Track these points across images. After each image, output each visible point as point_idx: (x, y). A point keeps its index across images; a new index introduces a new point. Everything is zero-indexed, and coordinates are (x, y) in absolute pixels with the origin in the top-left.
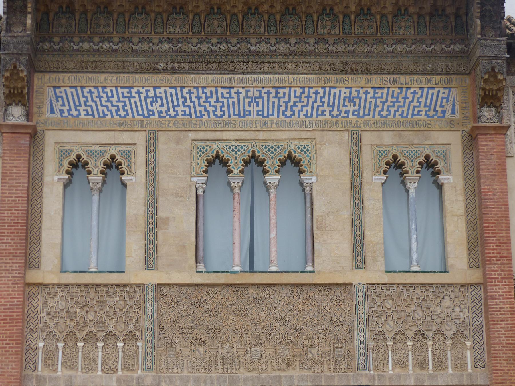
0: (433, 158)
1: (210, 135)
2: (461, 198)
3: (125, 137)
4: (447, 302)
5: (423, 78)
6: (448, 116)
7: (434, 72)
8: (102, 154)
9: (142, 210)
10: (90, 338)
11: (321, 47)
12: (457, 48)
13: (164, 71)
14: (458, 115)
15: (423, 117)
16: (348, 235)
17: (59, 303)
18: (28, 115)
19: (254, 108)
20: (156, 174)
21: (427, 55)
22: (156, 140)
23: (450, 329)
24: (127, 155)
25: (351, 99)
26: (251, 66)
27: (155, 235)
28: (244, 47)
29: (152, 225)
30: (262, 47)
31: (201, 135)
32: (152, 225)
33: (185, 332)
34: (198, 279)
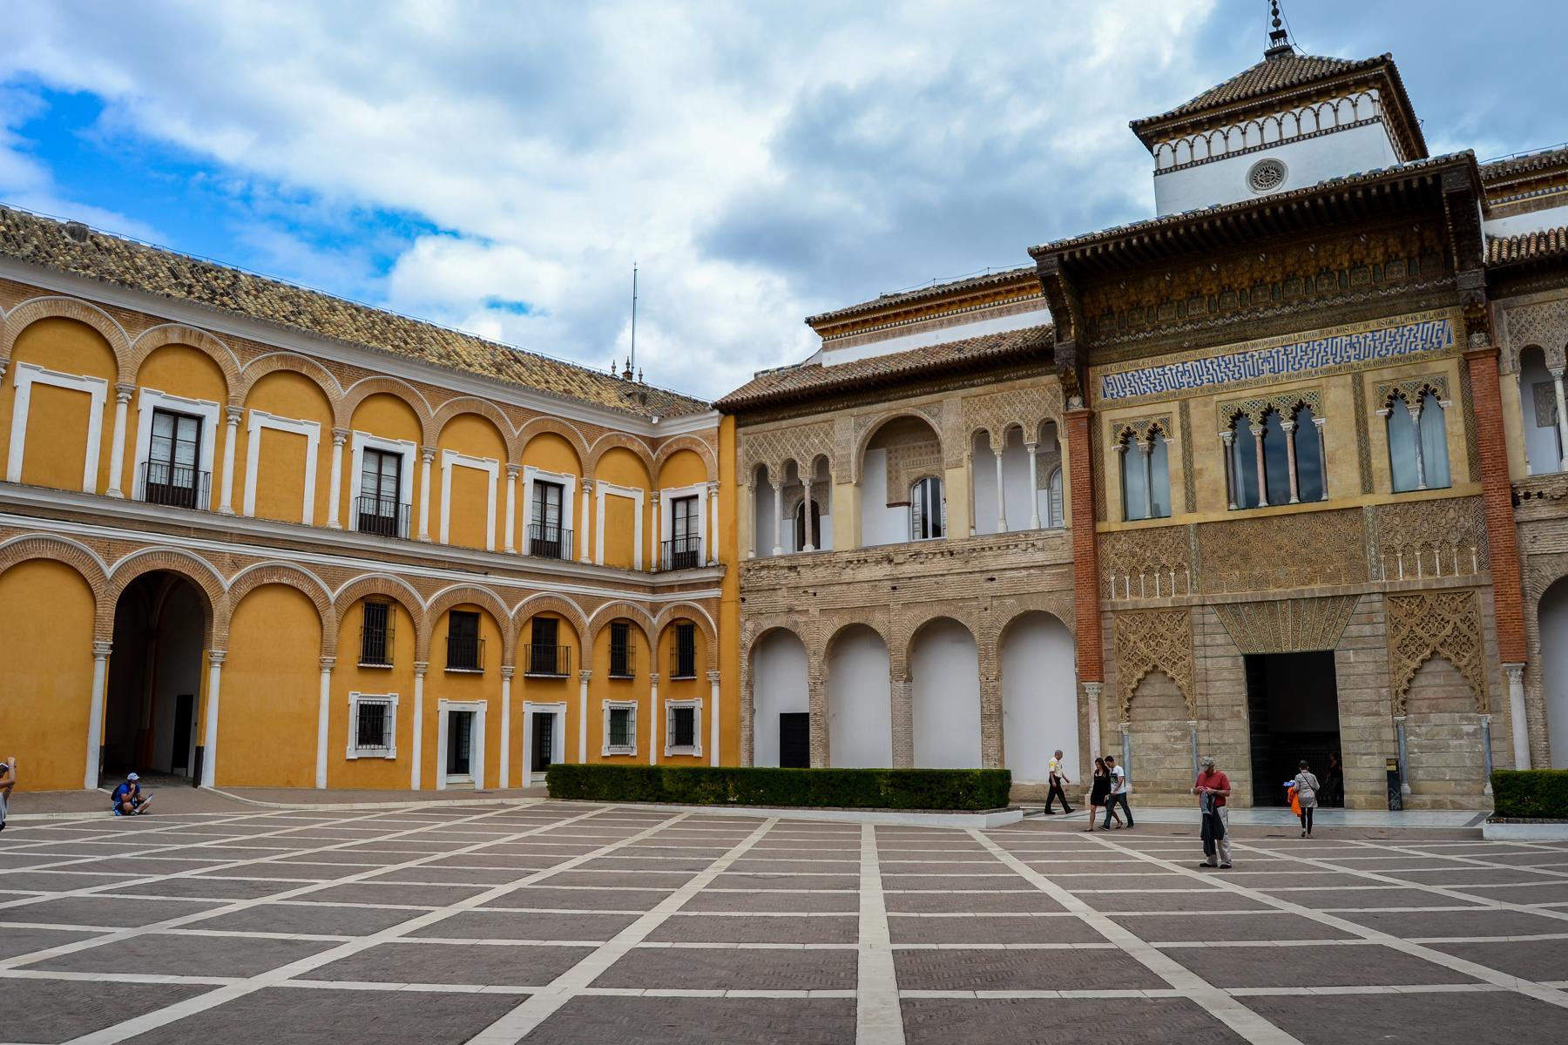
1: (1231, 396)
2: (1461, 419)
3: (1162, 408)
4: (1452, 514)
5: (1418, 315)
6: (1445, 345)
7: (1428, 308)
8: (1146, 424)
9: (1181, 465)
10: (1149, 571)
11: (1321, 304)
12: (1449, 281)
13: (1189, 348)
14: (1453, 343)
15: (1420, 350)
16: (1356, 464)
17: (1123, 545)
18: (1086, 403)
19: (1266, 367)
20: (1190, 434)
21: (1420, 293)
22: (1187, 406)
23: (1454, 538)
24: (1166, 422)
25: (1352, 345)
26: (1262, 331)
27: (1193, 484)
28: (1253, 316)
29: (1190, 475)
30: (1270, 313)
31: (1224, 397)
32: (1190, 475)
33: (1223, 559)
34: (1230, 516)
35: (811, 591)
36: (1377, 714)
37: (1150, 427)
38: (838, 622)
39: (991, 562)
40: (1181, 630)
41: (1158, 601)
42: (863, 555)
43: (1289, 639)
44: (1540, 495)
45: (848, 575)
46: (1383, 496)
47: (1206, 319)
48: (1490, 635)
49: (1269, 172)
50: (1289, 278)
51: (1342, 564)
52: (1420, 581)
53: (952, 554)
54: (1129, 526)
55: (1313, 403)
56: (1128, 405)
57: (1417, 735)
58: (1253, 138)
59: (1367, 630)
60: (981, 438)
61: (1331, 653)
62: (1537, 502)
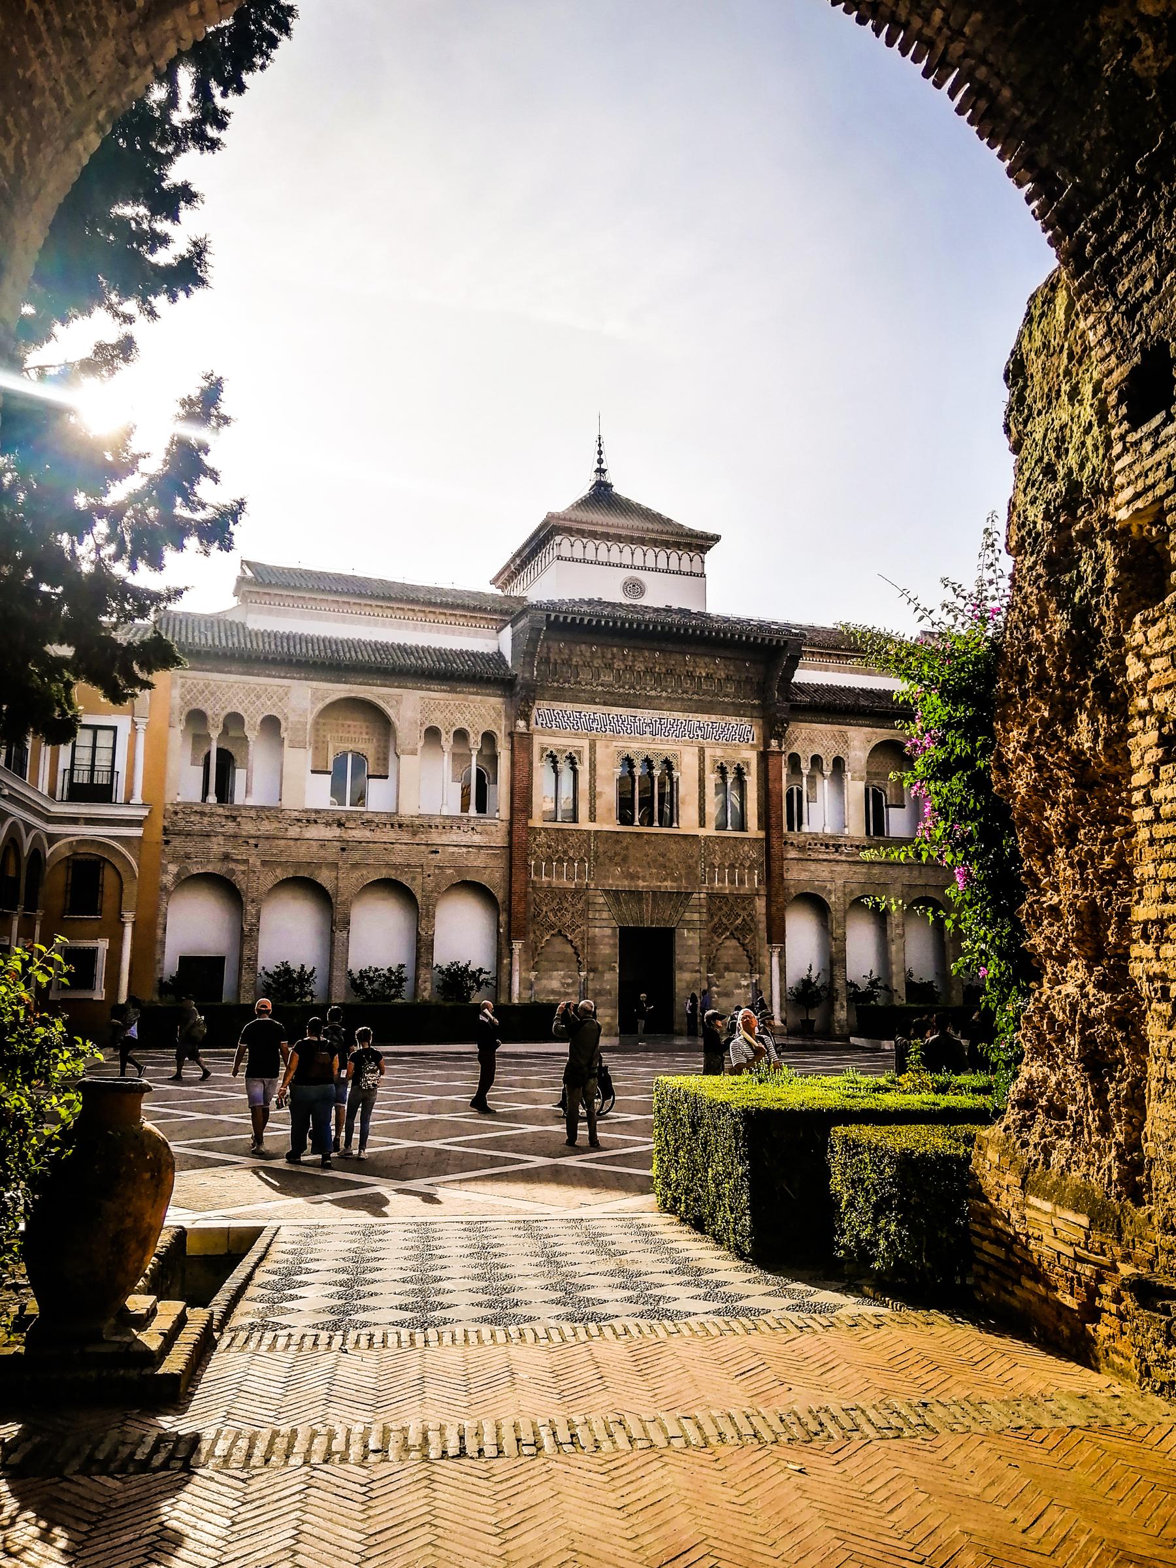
0: (742, 766)
1: (624, 744)
3: (577, 742)
4: (746, 848)
18: (528, 725)
19: (648, 729)
24: (579, 753)
28: (643, 692)
29: (593, 796)
30: (653, 693)
31: (620, 744)
32: (593, 796)
33: (611, 859)
35: (252, 841)
36: (698, 971)
37: (567, 754)
38: (281, 874)
39: (436, 838)
40: (579, 906)
41: (564, 882)
42: (313, 816)
43: (649, 917)
44: (792, 844)
45: (294, 832)
46: (710, 831)
47: (612, 686)
48: (762, 926)
49: (634, 587)
50: (670, 672)
51: (683, 872)
52: (727, 888)
53: (400, 826)
54: (548, 825)
55: (674, 761)
56: (553, 735)
57: (718, 986)
58: (626, 559)
59: (696, 916)
60: (432, 734)
61: (671, 931)
62: (790, 848)
